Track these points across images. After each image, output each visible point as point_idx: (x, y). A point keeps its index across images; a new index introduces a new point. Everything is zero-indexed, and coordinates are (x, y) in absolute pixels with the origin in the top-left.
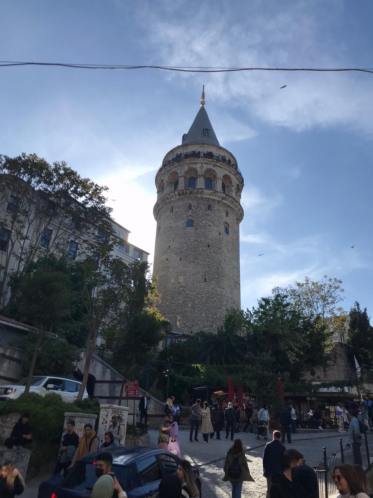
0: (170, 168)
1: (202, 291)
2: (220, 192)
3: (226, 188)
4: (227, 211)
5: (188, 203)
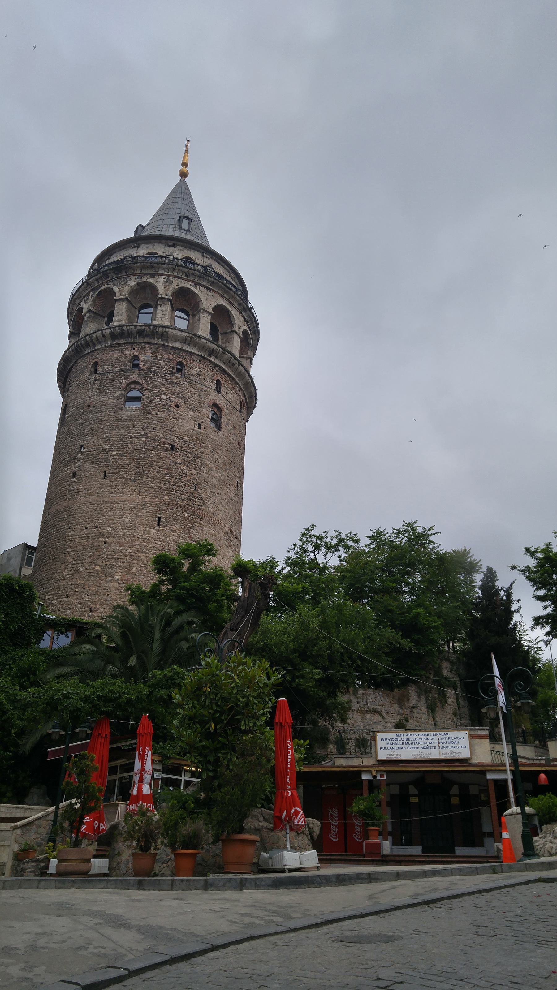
1: (150, 545)
2: (205, 339)
4: (218, 381)
5: (132, 355)
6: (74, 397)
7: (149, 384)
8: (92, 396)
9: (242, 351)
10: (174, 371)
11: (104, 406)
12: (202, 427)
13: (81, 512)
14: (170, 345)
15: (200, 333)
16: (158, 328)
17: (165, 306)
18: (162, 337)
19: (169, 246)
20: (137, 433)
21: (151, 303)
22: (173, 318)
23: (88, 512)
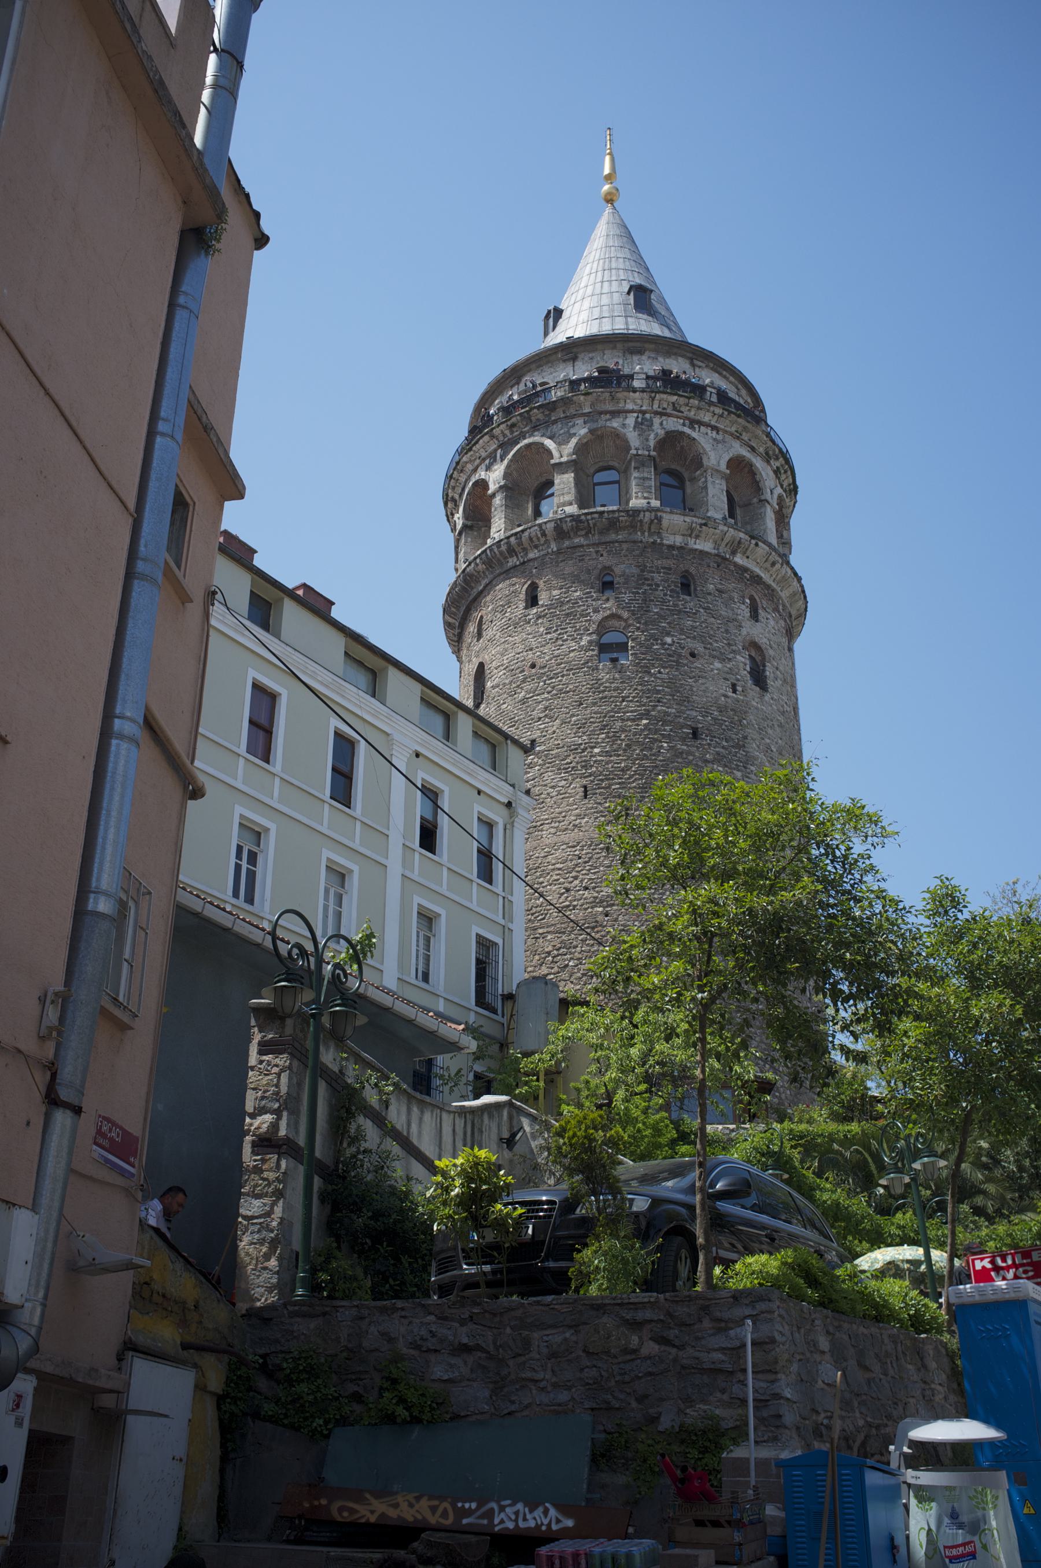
4: (752, 598)
5: (600, 566)
7: (638, 618)
8: (537, 647)
10: (678, 589)
11: (563, 665)
12: (739, 688)
13: (553, 861)
16: (642, 513)
17: (646, 470)
20: (632, 712)
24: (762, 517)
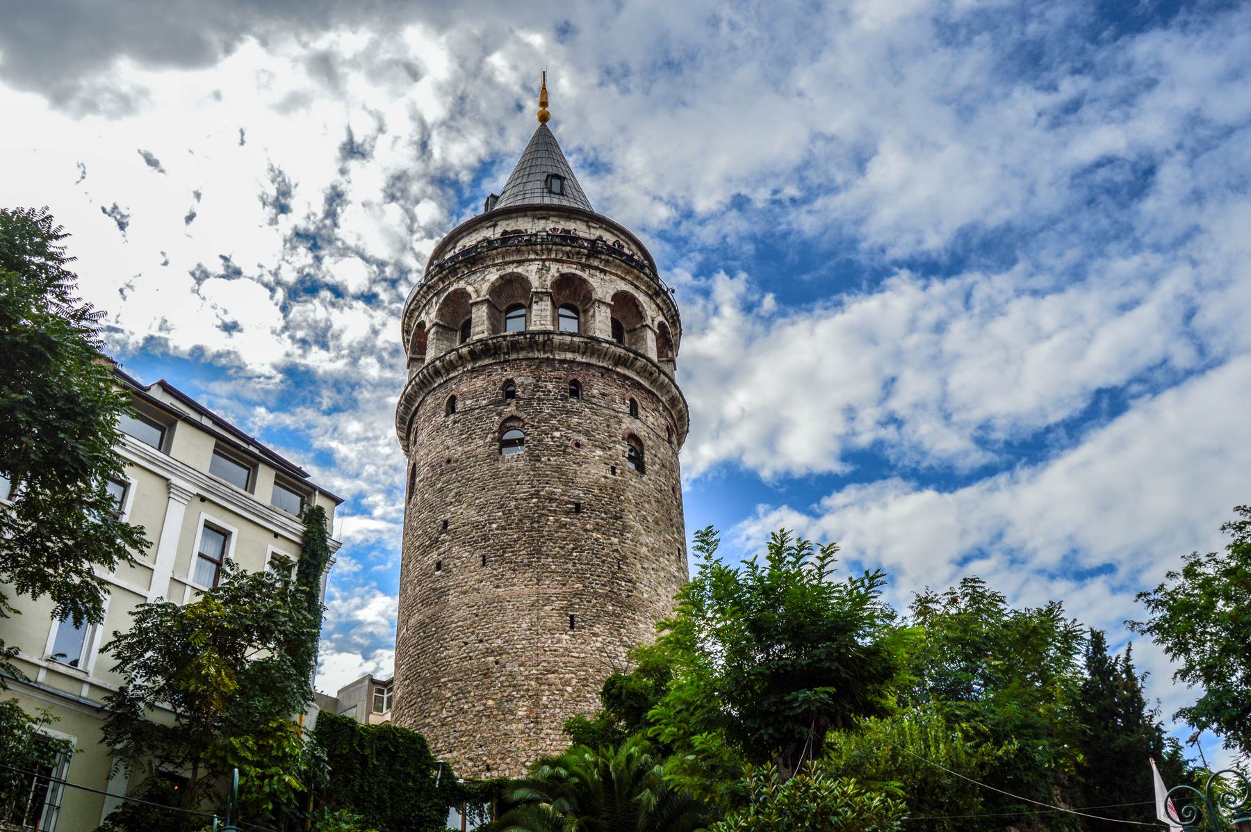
0: (444, 282)
1: (563, 659)
2: (607, 342)
3: (626, 335)
4: (632, 400)
6: (426, 451)
9: (660, 353)
12: (618, 471)
14: (557, 357)
15: (598, 335)
18: (544, 347)
19: (539, 219)
21: (523, 302)
22: (555, 320)
23: (466, 619)
24: (644, 339)
